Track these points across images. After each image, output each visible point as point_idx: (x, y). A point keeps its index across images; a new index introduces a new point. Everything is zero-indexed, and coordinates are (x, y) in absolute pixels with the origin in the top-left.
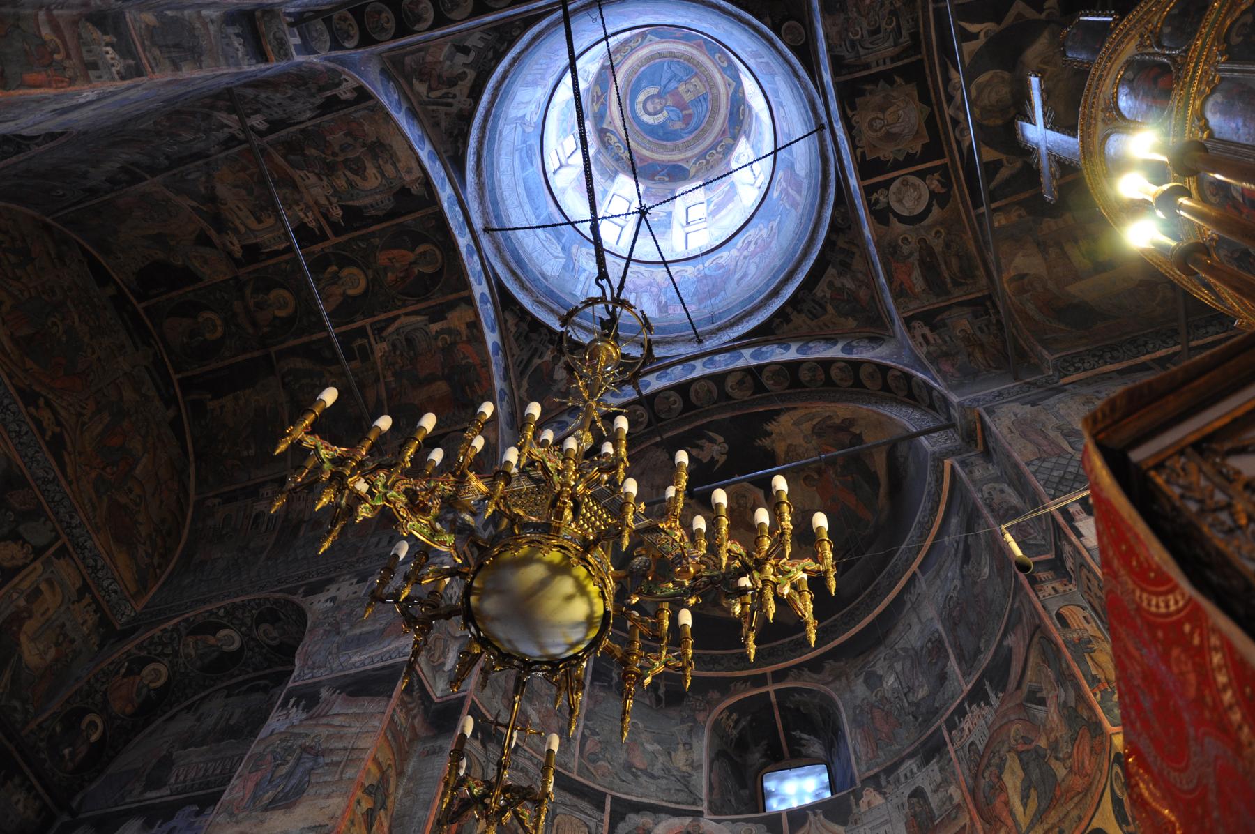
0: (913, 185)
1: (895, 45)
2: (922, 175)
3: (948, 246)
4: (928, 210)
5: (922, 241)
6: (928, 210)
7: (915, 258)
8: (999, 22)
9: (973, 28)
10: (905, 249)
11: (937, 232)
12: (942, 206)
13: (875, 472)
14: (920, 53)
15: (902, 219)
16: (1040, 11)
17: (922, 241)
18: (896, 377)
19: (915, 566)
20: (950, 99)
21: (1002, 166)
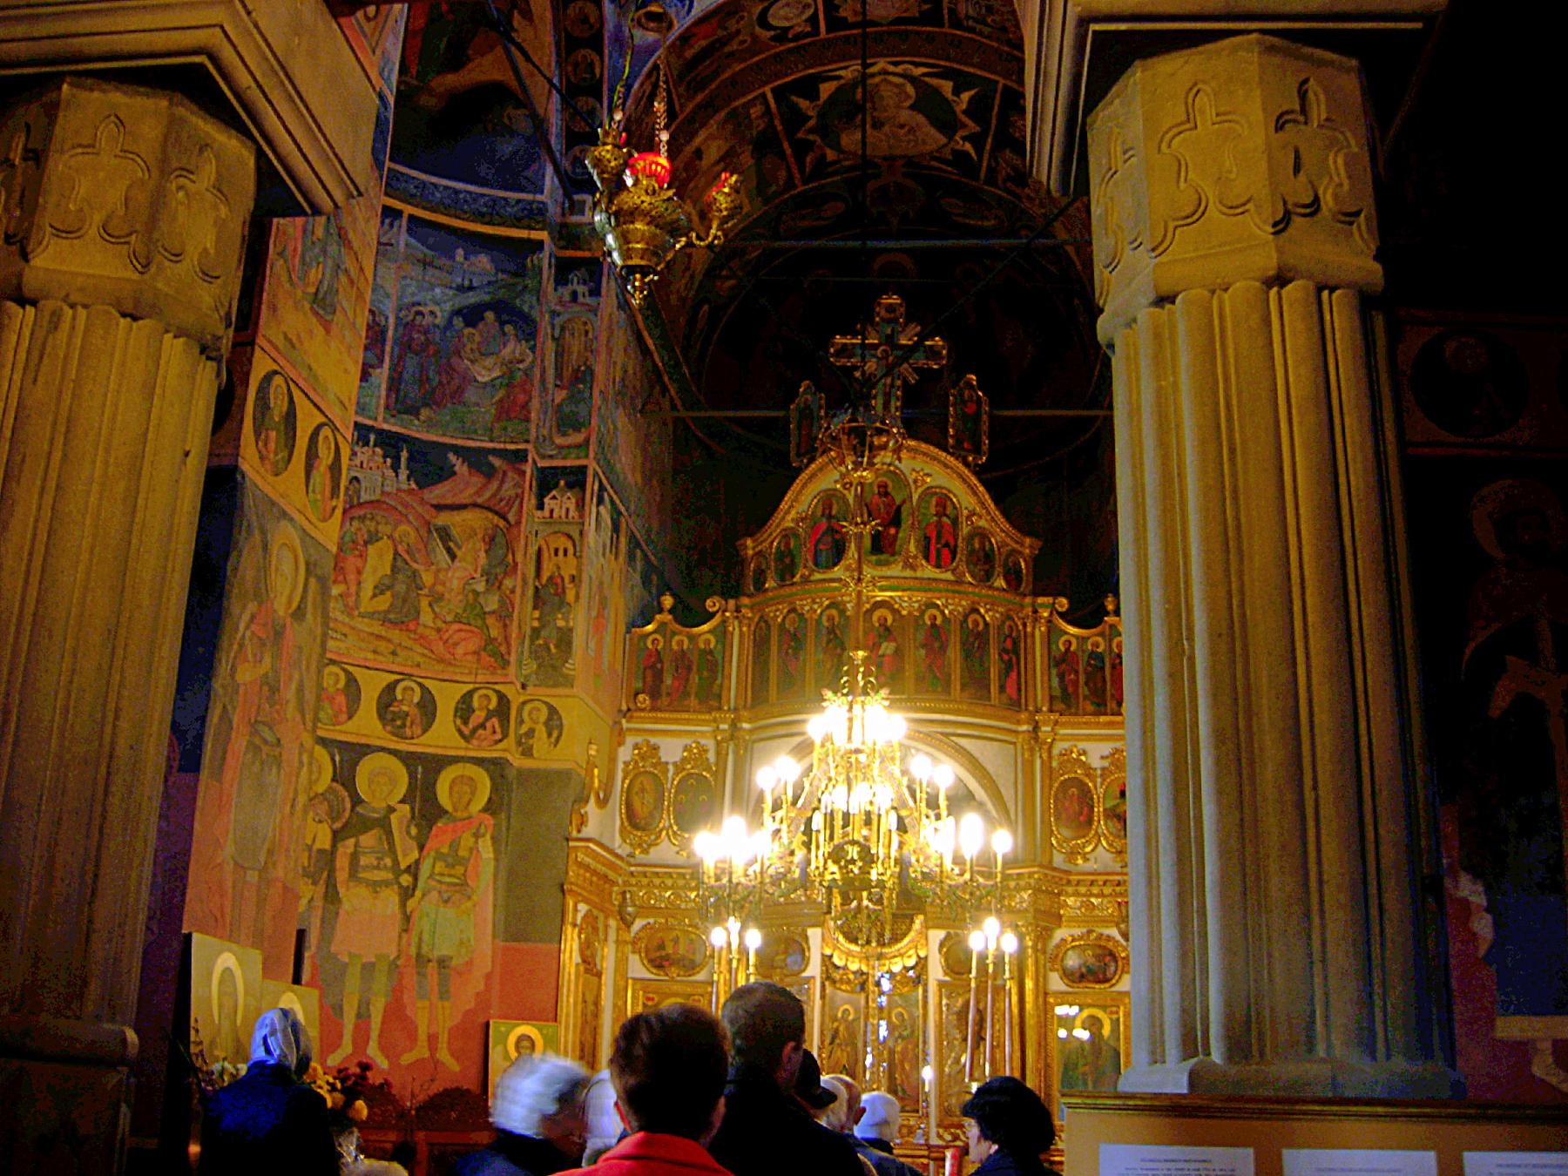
0: (802, 13)
1: (968, 17)
2: (813, 20)
3: (732, 54)
4: (770, 27)
5: (738, 32)
6: (770, 27)
7: (721, 33)
8: (964, 112)
9: (966, 96)
10: (732, 25)
11: (745, 41)
12: (773, 38)
13: (470, 60)
14: (950, 27)
15: (765, 11)
16: (964, 138)
17: (738, 32)
18: (592, 65)
19: (409, 210)
20: (896, 64)
21: (811, 101)
